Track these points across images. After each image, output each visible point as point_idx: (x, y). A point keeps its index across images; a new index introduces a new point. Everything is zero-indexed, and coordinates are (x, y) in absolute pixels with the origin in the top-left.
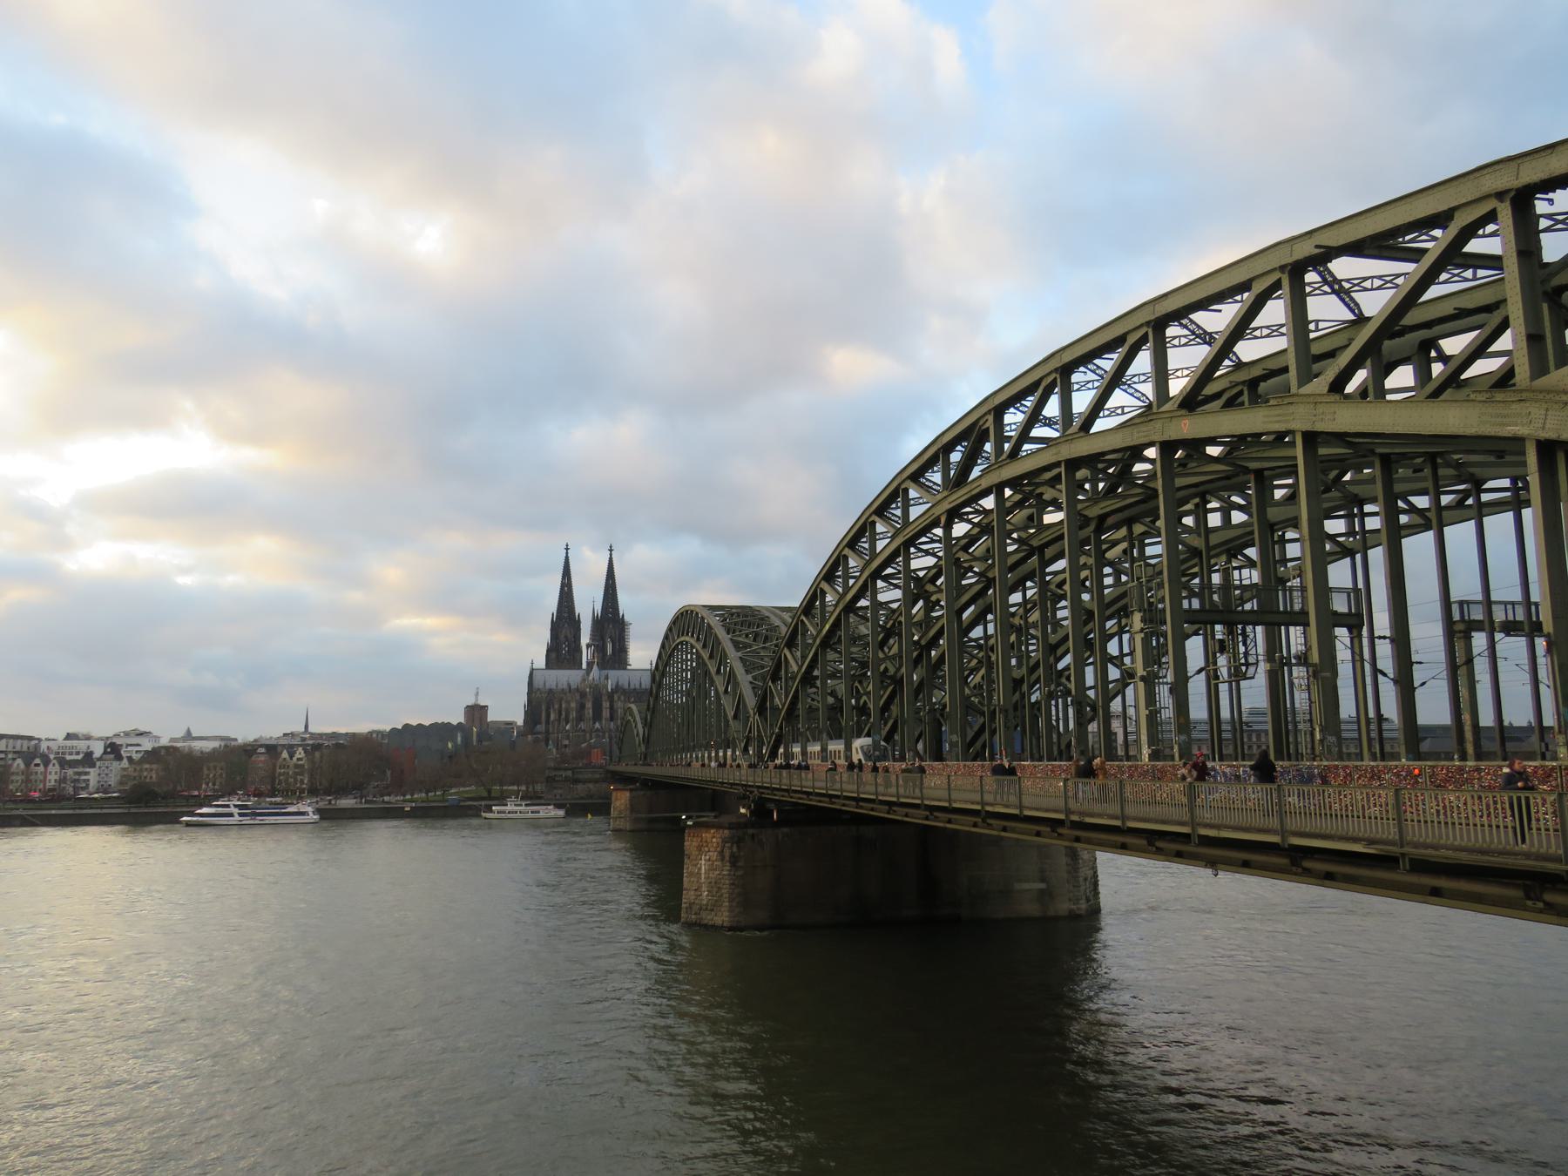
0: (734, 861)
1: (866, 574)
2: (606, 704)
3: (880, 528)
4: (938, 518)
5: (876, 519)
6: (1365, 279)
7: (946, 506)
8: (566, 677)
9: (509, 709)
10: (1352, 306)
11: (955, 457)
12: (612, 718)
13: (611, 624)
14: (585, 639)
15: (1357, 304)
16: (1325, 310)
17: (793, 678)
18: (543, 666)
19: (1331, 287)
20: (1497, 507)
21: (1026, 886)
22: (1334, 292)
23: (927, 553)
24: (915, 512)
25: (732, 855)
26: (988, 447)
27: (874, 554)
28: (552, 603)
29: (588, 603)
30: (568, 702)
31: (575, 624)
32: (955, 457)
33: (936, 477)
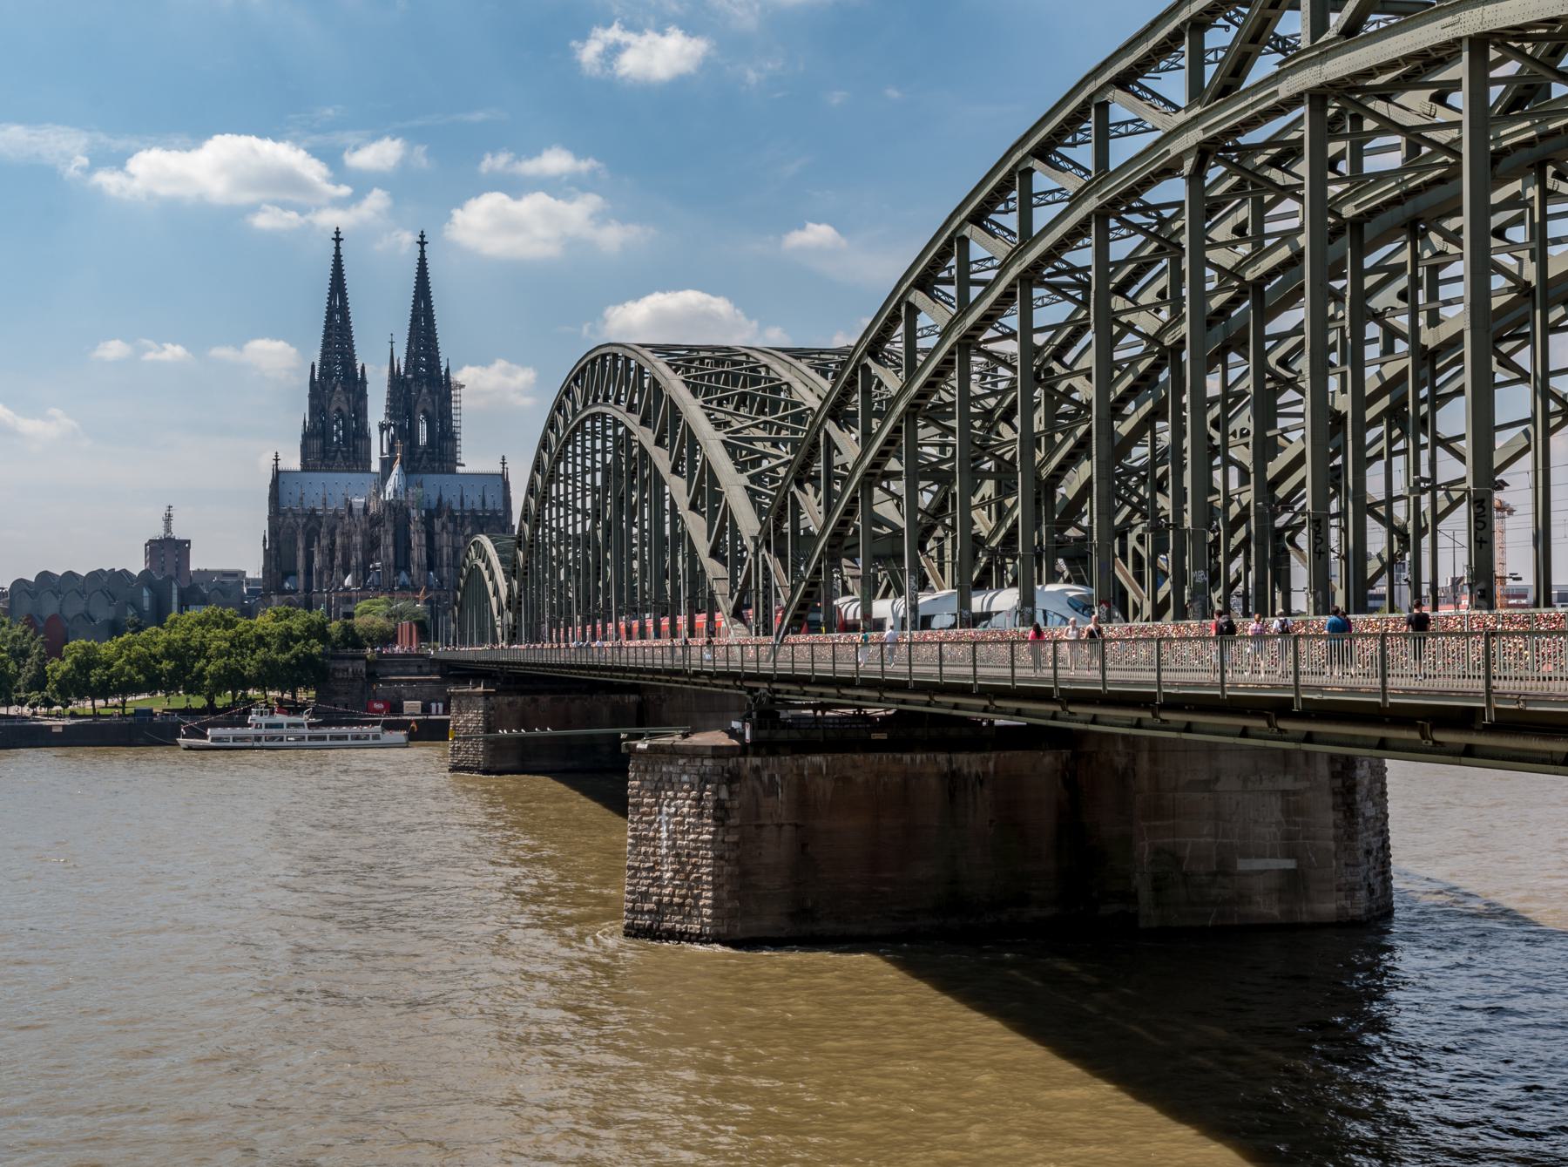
0: (722, 814)
1: (1014, 271)
2: (417, 539)
4: (1180, 158)
5: (1036, 164)
7: (1195, 136)
9: (233, 545)
11: (1219, 38)
12: (431, 565)
17: (845, 481)
18: (298, 468)
21: (1258, 864)
24: (1122, 150)
25: (719, 804)
27: (1027, 236)
30: (347, 535)
31: (356, 386)
33: (1172, 83)
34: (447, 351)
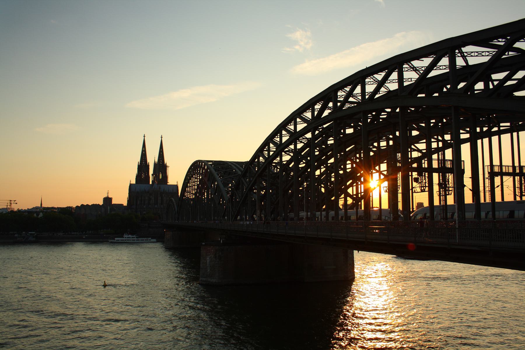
3: (284, 132)
6: (472, 52)
8: (143, 187)
9: (121, 198)
10: (466, 61)
11: (318, 107)
13: (161, 166)
14: (151, 172)
15: (467, 61)
16: (460, 62)
19: (461, 54)
20: (505, 132)
22: (461, 56)
23: (301, 142)
26: (331, 105)
28: (138, 159)
29: (152, 159)
31: (148, 167)
32: (318, 107)
34: (167, 160)
